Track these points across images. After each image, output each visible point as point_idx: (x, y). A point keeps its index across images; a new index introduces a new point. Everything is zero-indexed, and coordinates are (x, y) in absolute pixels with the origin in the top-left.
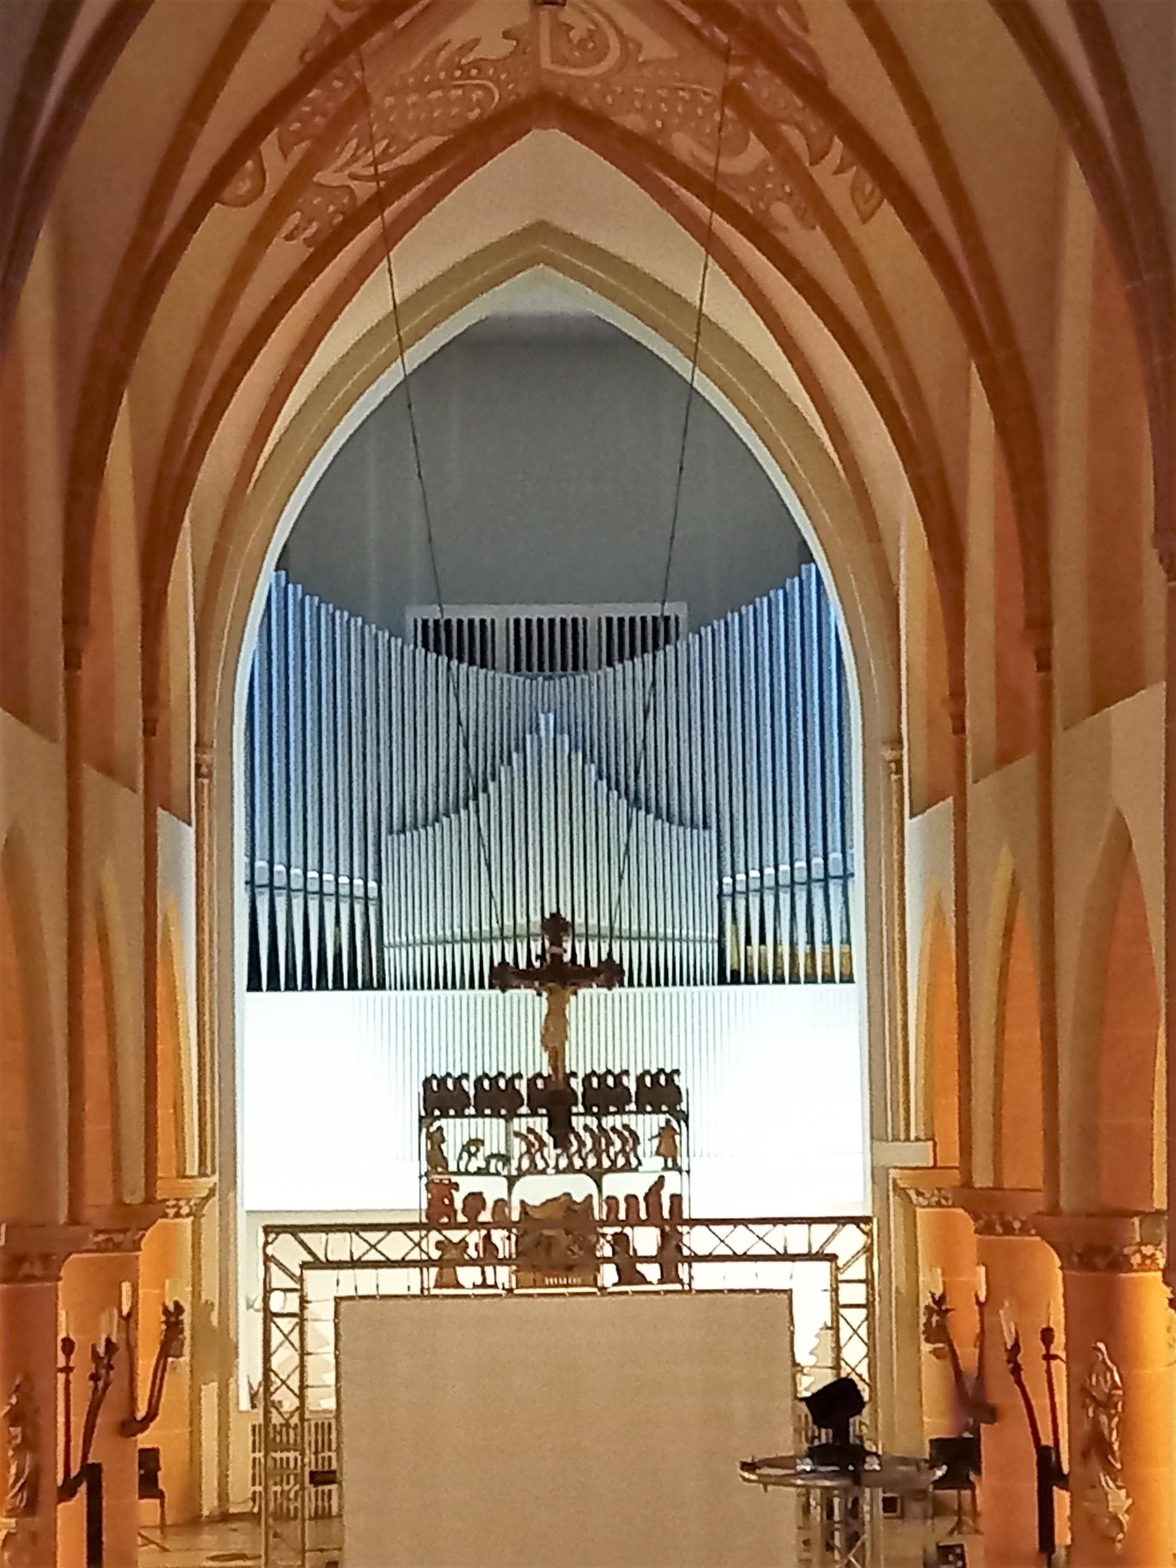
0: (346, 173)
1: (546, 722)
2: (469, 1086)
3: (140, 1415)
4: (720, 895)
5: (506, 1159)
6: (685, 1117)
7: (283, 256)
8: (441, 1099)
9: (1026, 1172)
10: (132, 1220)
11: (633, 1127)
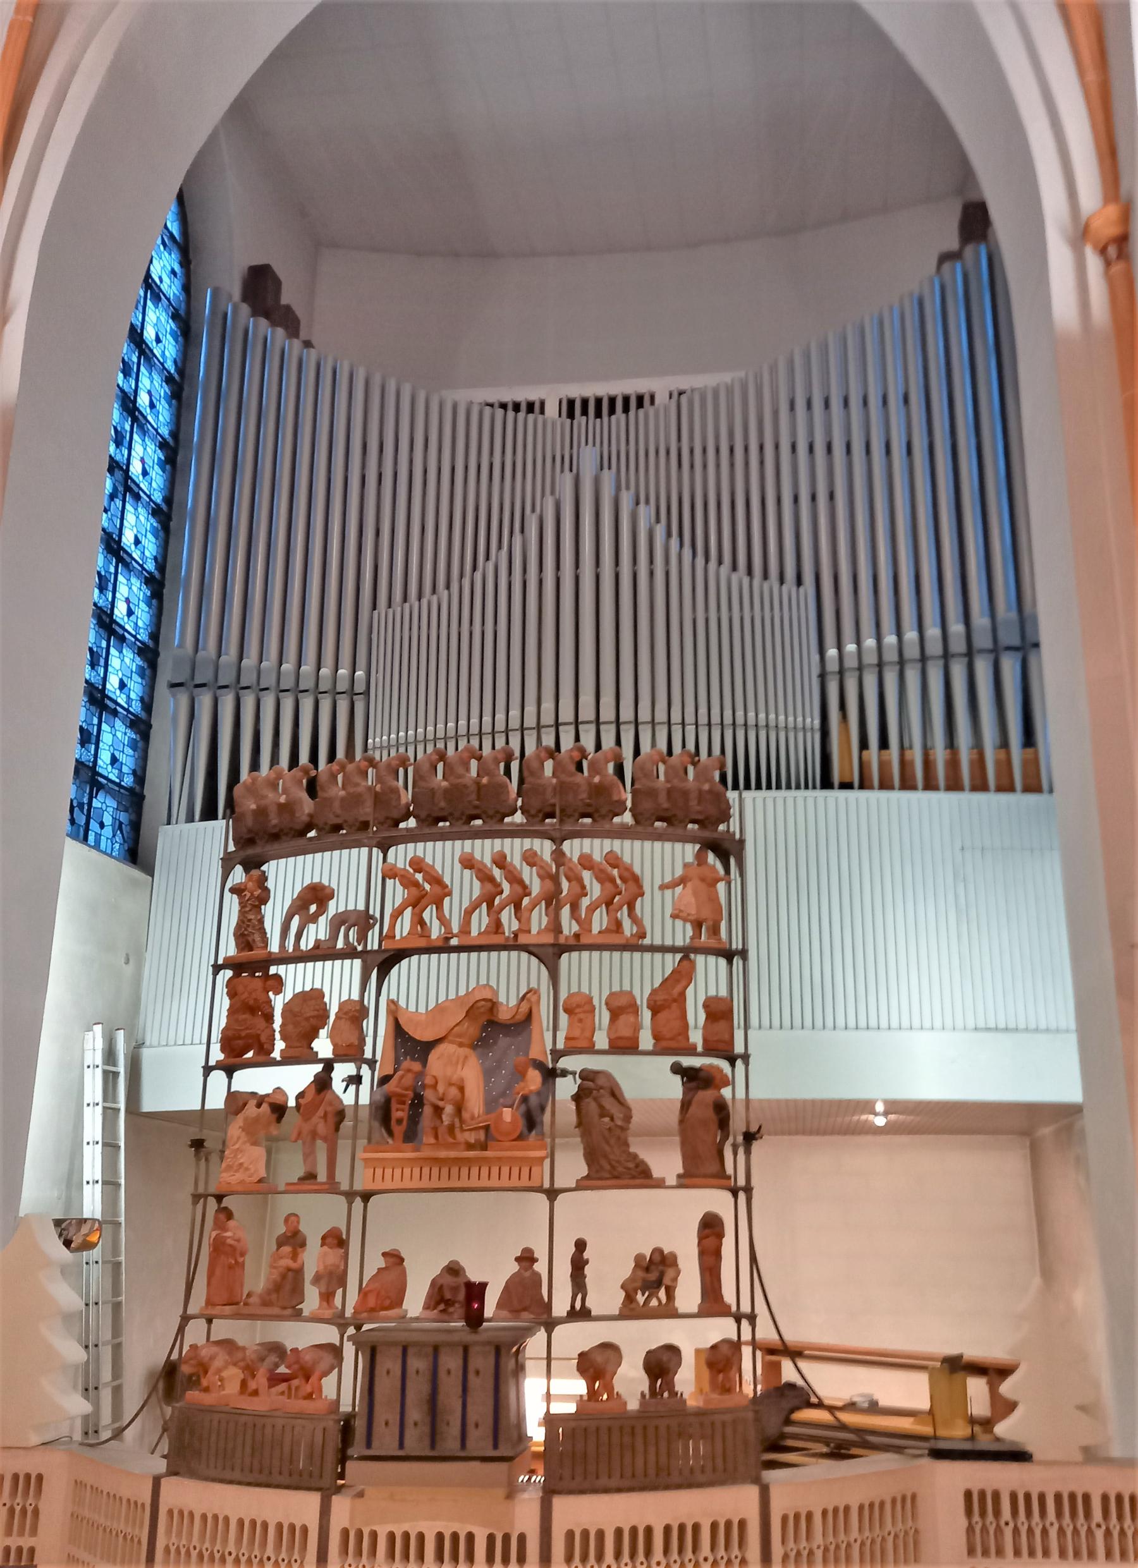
4: (823, 676)
5: (364, 921)
11: (627, 859)
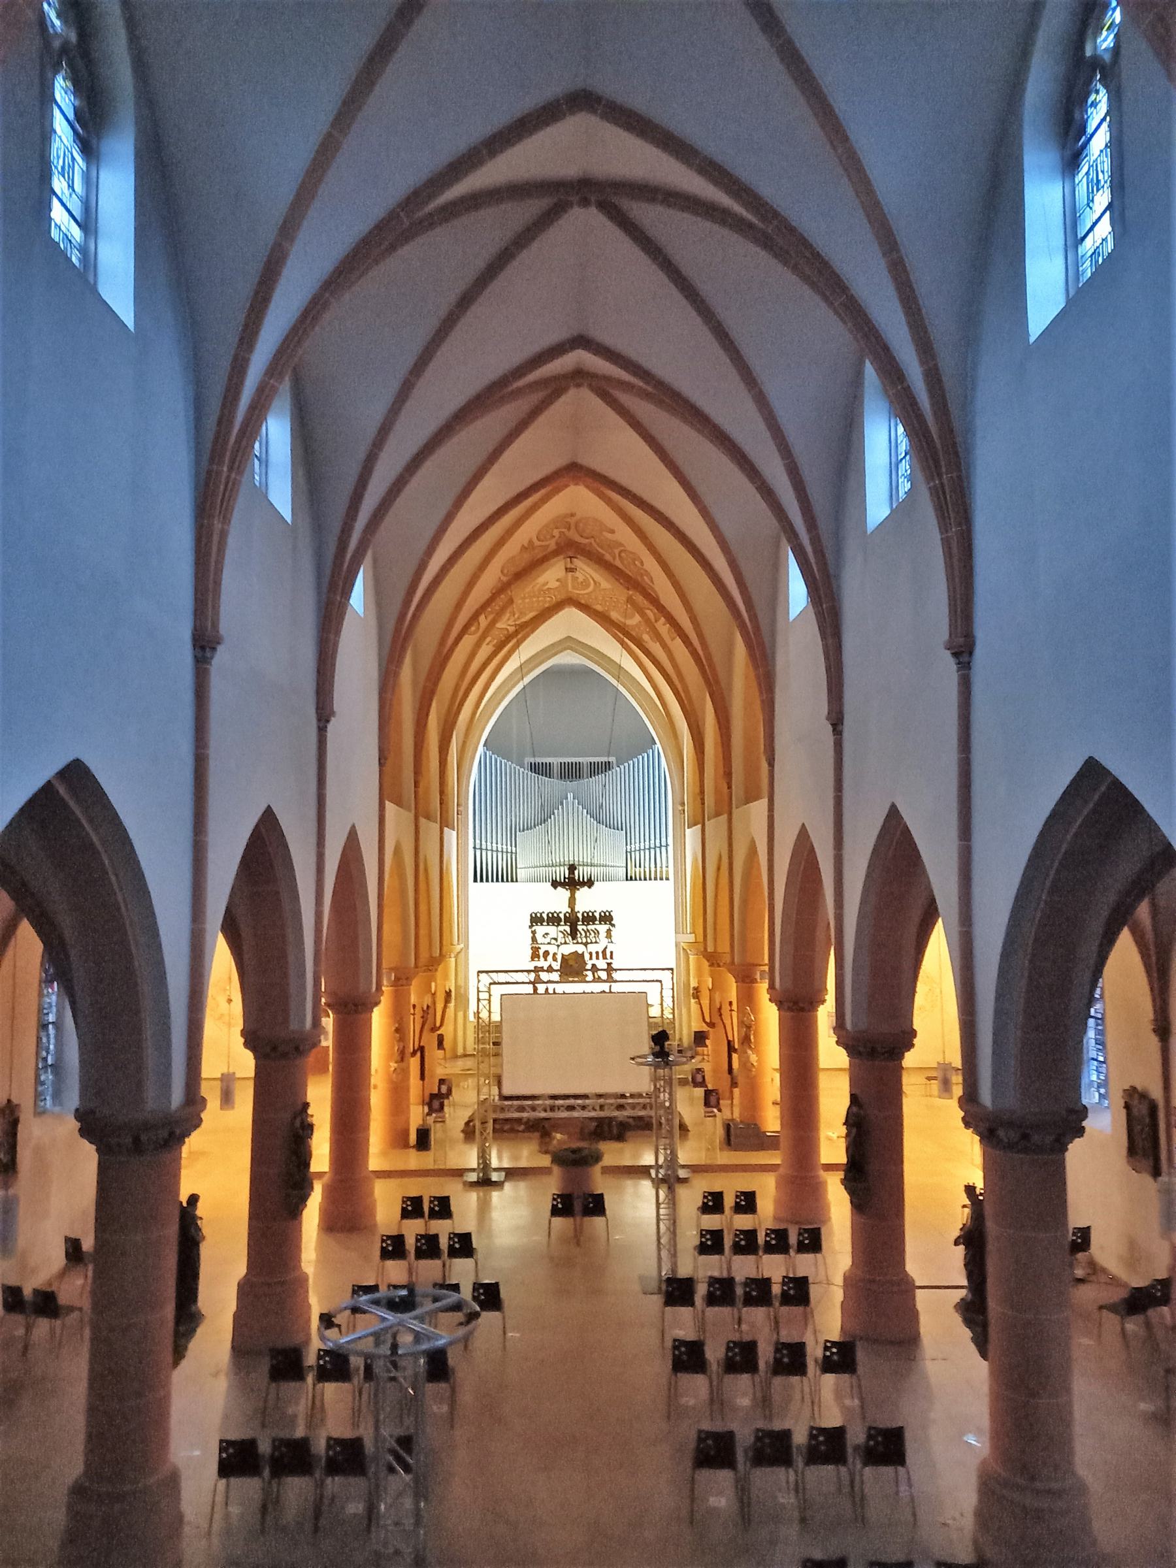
0: (506, 624)
2: (545, 916)
3: (438, 1024)
7: (485, 651)
8: (536, 920)
9: (724, 947)
10: (434, 963)
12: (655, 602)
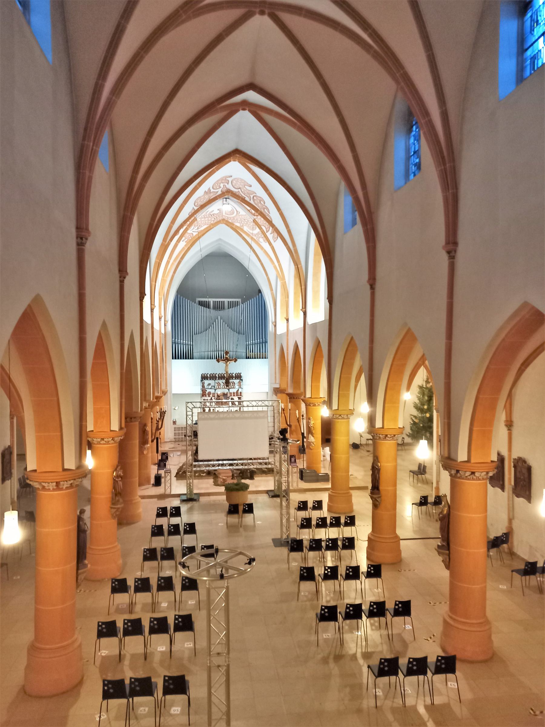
1: (219, 318)
2: (208, 375)
6: (242, 380)
8: (204, 377)
12: (270, 223)
